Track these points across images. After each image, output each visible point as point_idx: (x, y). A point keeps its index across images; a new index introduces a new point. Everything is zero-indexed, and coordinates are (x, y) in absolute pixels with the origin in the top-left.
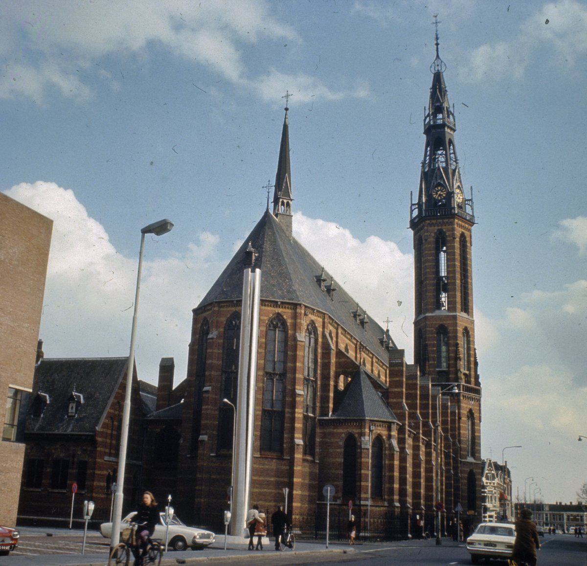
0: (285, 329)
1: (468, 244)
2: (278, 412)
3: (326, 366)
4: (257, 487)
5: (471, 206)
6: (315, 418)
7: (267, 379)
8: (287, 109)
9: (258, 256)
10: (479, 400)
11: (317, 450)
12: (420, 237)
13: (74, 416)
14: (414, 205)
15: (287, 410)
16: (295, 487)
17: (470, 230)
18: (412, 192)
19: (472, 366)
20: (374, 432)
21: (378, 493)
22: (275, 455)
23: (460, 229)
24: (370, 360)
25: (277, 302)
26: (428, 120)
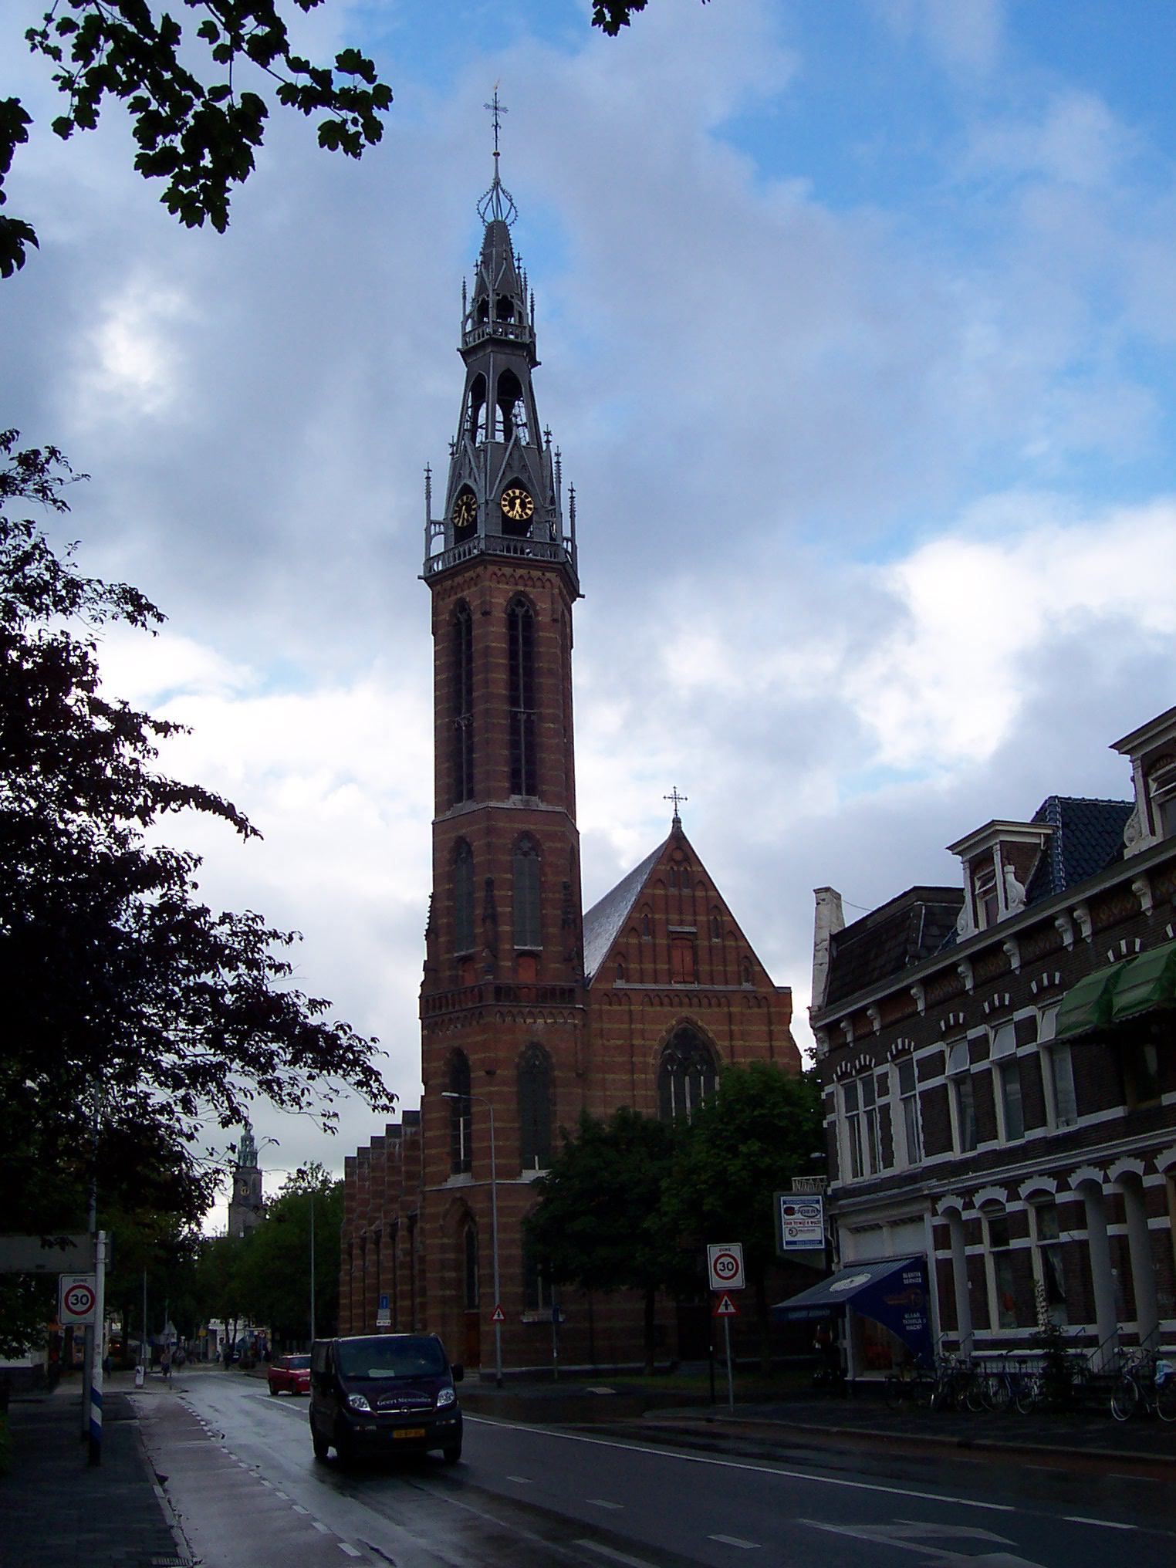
12: (462, 606)
14: (435, 523)
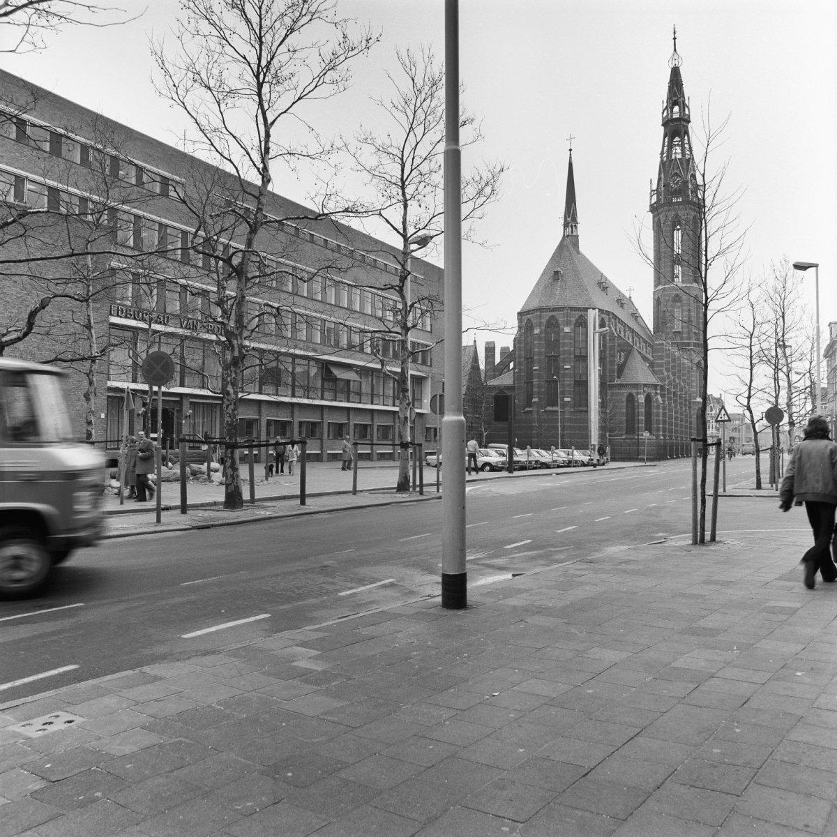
8: (570, 150)
12: (659, 220)
14: (653, 191)
26: (665, 114)
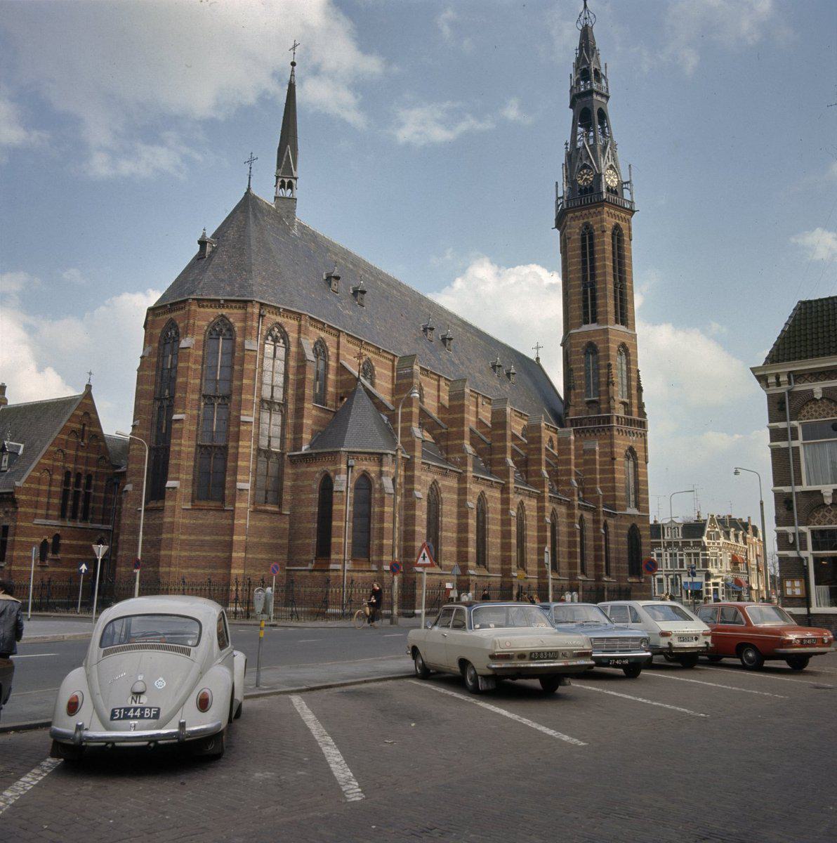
0: (232, 338)
1: (626, 238)
2: (219, 448)
3: (300, 384)
4: (186, 550)
5: (629, 190)
6: (283, 454)
7: (206, 404)
8: (293, 64)
9: (216, 248)
10: (645, 435)
11: (287, 497)
13: (6, 471)
15: (231, 444)
16: (235, 547)
17: (629, 221)
18: (557, 183)
19: (634, 392)
20: (356, 468)
21: (363, 549)
22: (212, 504)
23: (613, 220)
24: (436, 383)
25: (219, 300)
